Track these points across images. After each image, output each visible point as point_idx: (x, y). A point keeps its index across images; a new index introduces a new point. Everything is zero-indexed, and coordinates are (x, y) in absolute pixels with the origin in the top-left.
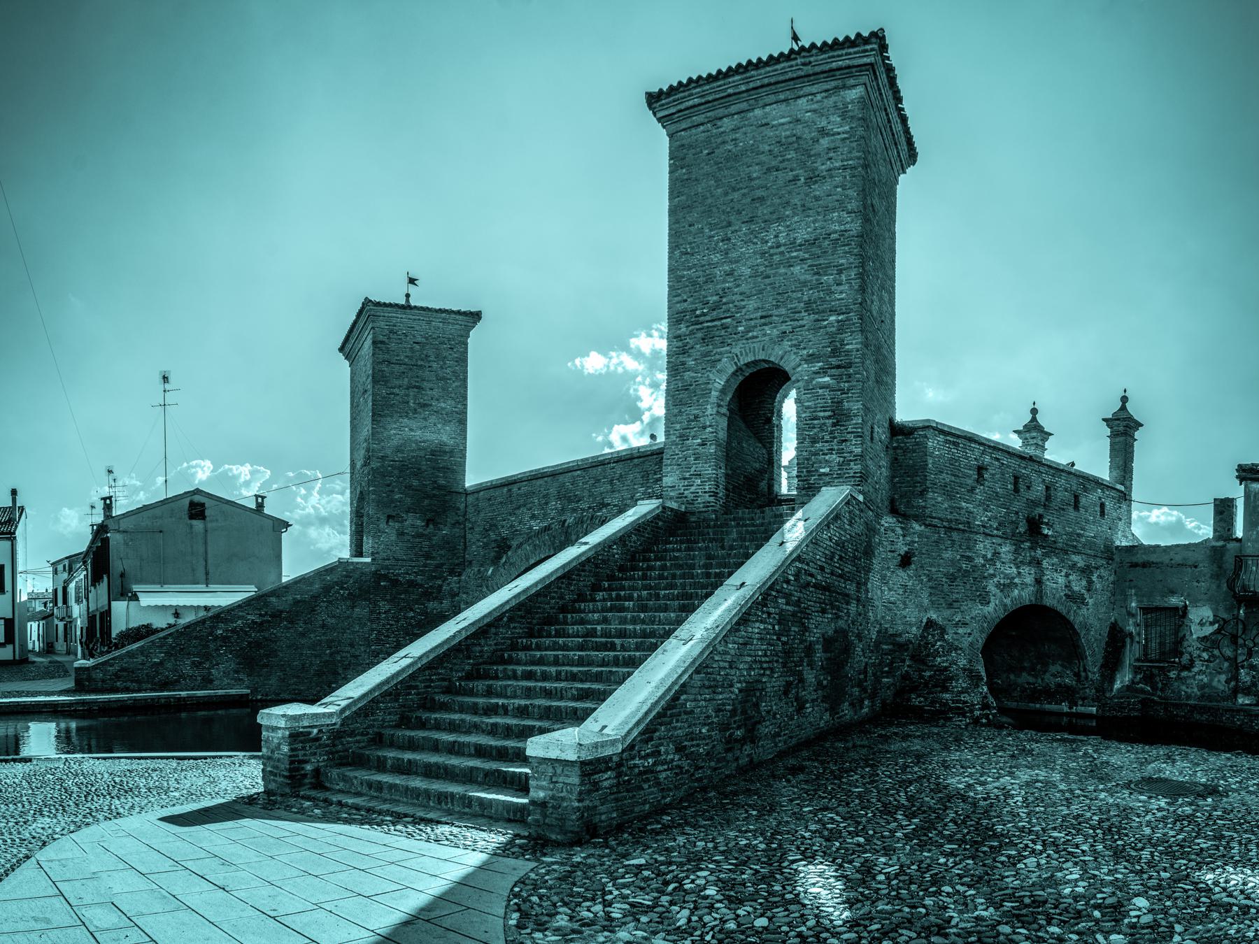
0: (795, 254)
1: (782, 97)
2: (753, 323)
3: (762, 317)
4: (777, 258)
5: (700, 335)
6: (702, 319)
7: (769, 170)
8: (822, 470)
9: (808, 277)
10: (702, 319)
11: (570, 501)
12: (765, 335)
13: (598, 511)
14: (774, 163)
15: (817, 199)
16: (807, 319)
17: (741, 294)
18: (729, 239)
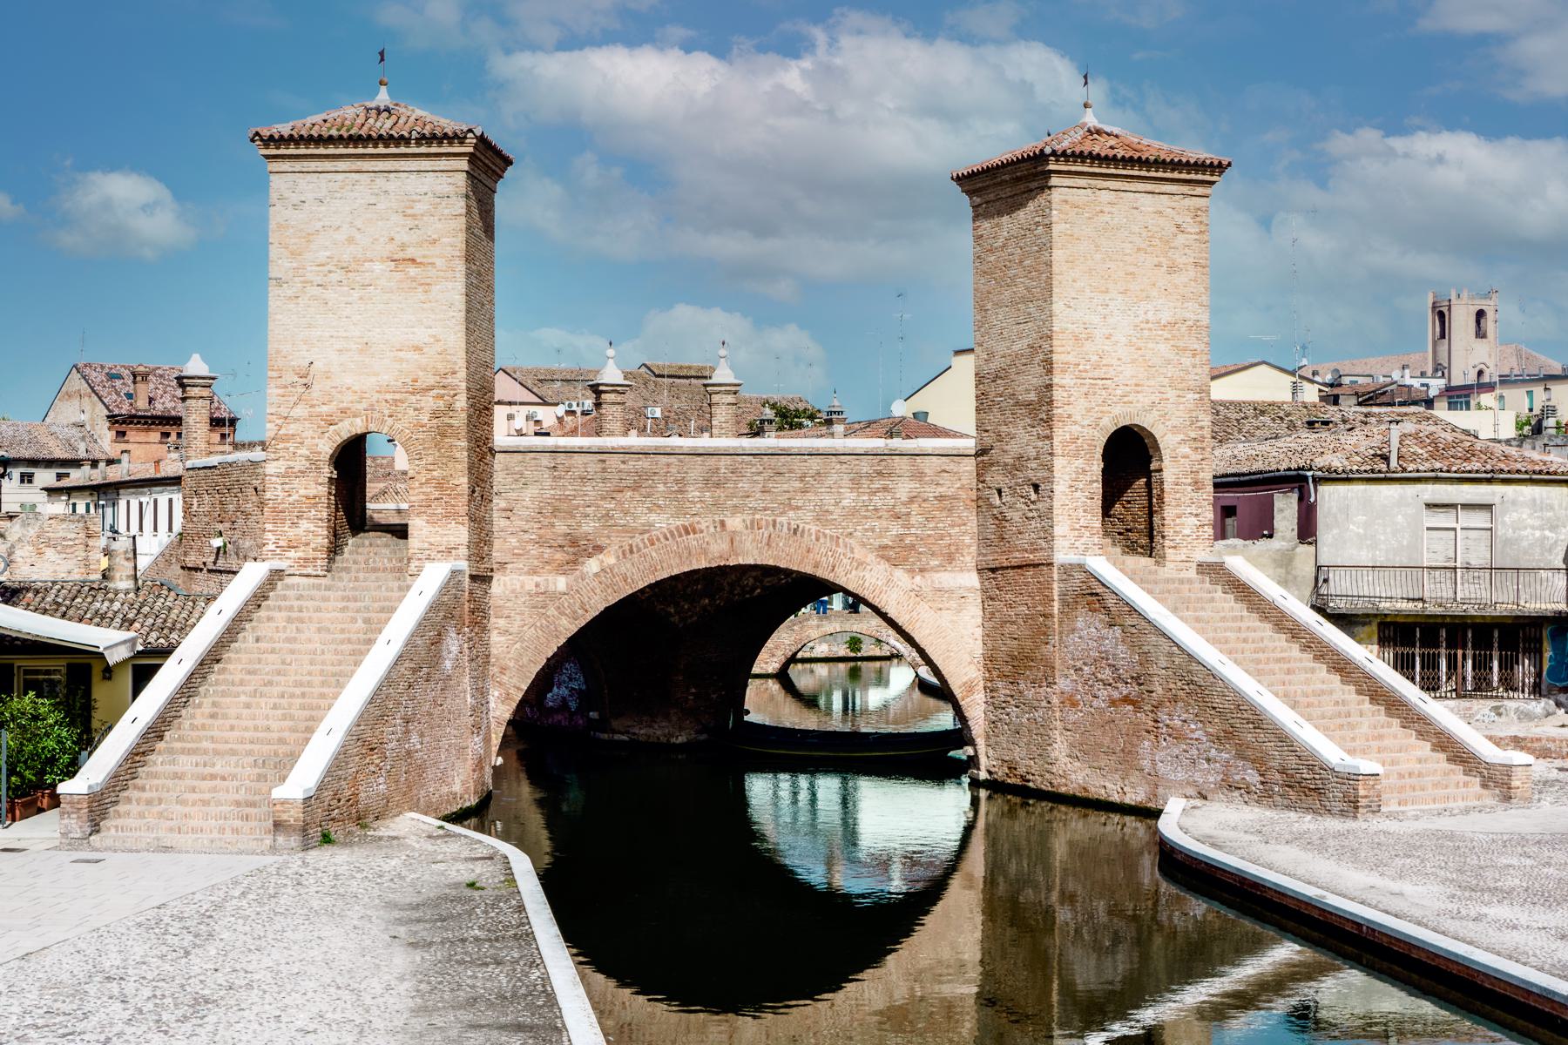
0: (1161, 332)
2: (1128, 389)
3: (1136, 385)
4: (1146, 333)
5: (1085, 389)
6: (1084, 375)
7: (1139, 249)
8: (1187, 532)
9: (1172, 357)
10: (1084, 375)
12: (1138, 401)
14: (1142, 246)
15: (1176, 287)
16: (1171, 394)
17: (1119, 359)
18: (1107, 305)
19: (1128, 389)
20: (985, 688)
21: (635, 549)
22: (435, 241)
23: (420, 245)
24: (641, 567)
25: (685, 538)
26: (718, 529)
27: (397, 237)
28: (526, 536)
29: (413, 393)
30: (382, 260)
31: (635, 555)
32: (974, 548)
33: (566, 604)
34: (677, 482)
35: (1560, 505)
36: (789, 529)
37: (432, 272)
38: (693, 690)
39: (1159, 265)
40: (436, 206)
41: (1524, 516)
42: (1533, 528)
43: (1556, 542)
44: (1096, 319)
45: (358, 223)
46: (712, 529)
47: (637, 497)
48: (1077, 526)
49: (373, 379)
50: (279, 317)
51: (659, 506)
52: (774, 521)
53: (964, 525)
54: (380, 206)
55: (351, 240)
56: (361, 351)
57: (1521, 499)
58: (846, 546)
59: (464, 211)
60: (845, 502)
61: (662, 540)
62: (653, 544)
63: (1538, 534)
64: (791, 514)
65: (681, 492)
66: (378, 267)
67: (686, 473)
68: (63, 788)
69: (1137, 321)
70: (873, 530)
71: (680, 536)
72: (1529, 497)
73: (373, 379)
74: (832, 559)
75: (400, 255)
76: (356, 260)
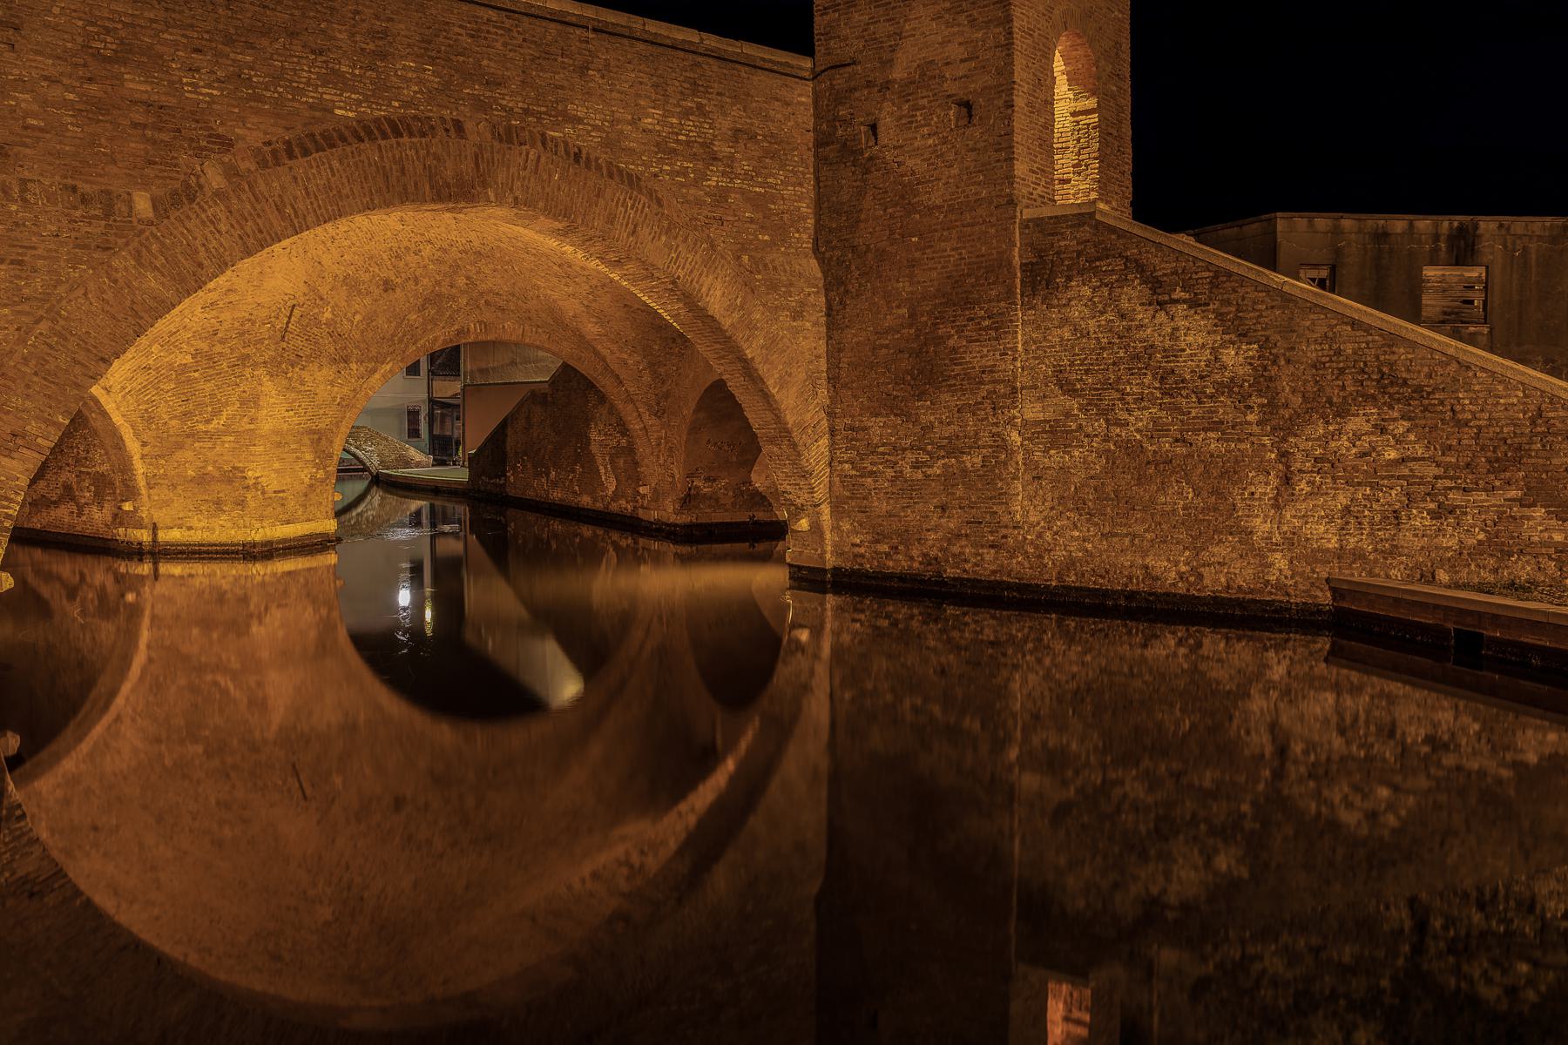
13: (556, 125)
20: (832, 432)
21: (297, 151)
24: (312, 187)
25: (393, 141)
26: (452, 133)
28: (55, 92)
31: (302, 161)
32: (811, 222)
33: (154, 247)
34: (374, 35)
36: (567, 153)
38: (277, 465)
46: (441, 133)
51: (342, 75)
52: (543, 135)
53: (801, 185)
58: (651, 195)
61: (351, 139)
62: (333, 146)
65: (383, 56)
67: (390, 20)
70: (683, 172)
71: (385, 136)
74: (633, 212)
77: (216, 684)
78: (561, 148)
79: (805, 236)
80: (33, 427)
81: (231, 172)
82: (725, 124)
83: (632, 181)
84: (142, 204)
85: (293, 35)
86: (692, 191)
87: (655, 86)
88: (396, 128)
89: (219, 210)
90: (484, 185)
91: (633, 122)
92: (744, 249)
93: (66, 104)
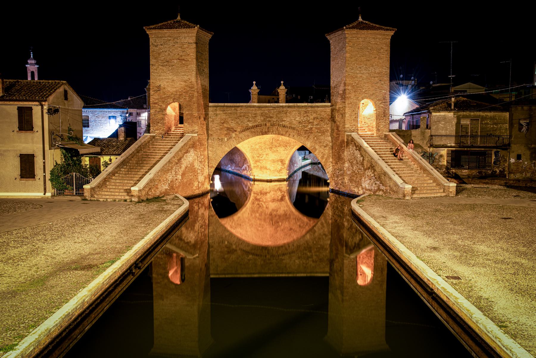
0: (376, 75)
1: (373, 37)
6: (354, 86)
8: (382, 126)
11: (267, 117)
19: (366, 90)
22: (189, 55)
23: (185, 56)
27: (180, 54)
29: (184, 92)
30: (177, 60)
32: (330, 131)
34: (254, 114)
35: (499, 119)
37: (188, 63)
38: (273, 166)
39: (376, 57)
40: (189, 46)
41: (488, 122)
42: (490, 124)
43: (497, 128)
44: (358, 72)
45: (171, 50)
47: (244, 118)
48: (352, 125)
49: (175, 89)
50: (153, 74)
52: (279, 124)
54: (176, 46)
55: (169, 54)
56: (171, 82)
57: (488, 117)
59: (195, 47)
60: (297, 119)
63: (492, 126)
64: (283, 122)
65: (255, 117)
66: (175, 61)
68: (84, 187)
69: (369, 72)
71: (255, 128)
72: (490, 116)
73: (175, 89)
75: (180, 58)
76: (170, 59)
77: (262, 204)
78: (282, 126)
79: (329, 133)
80: (214, 165)
81: (236, 135)
82: (312, 117)
83: (294, 129)
84: (226, 139)
85: (244, 116)
86: (305, 128)
87: (299, 113)
88: (257, 126)
89: (234, 139)
90: (269, 132)
91: (295, 119)
92: (316, 137)
93: (218, 129)
